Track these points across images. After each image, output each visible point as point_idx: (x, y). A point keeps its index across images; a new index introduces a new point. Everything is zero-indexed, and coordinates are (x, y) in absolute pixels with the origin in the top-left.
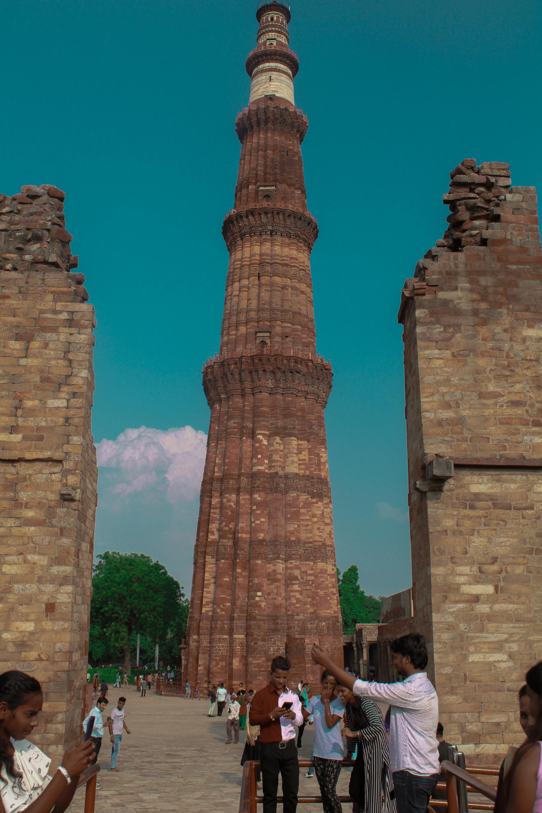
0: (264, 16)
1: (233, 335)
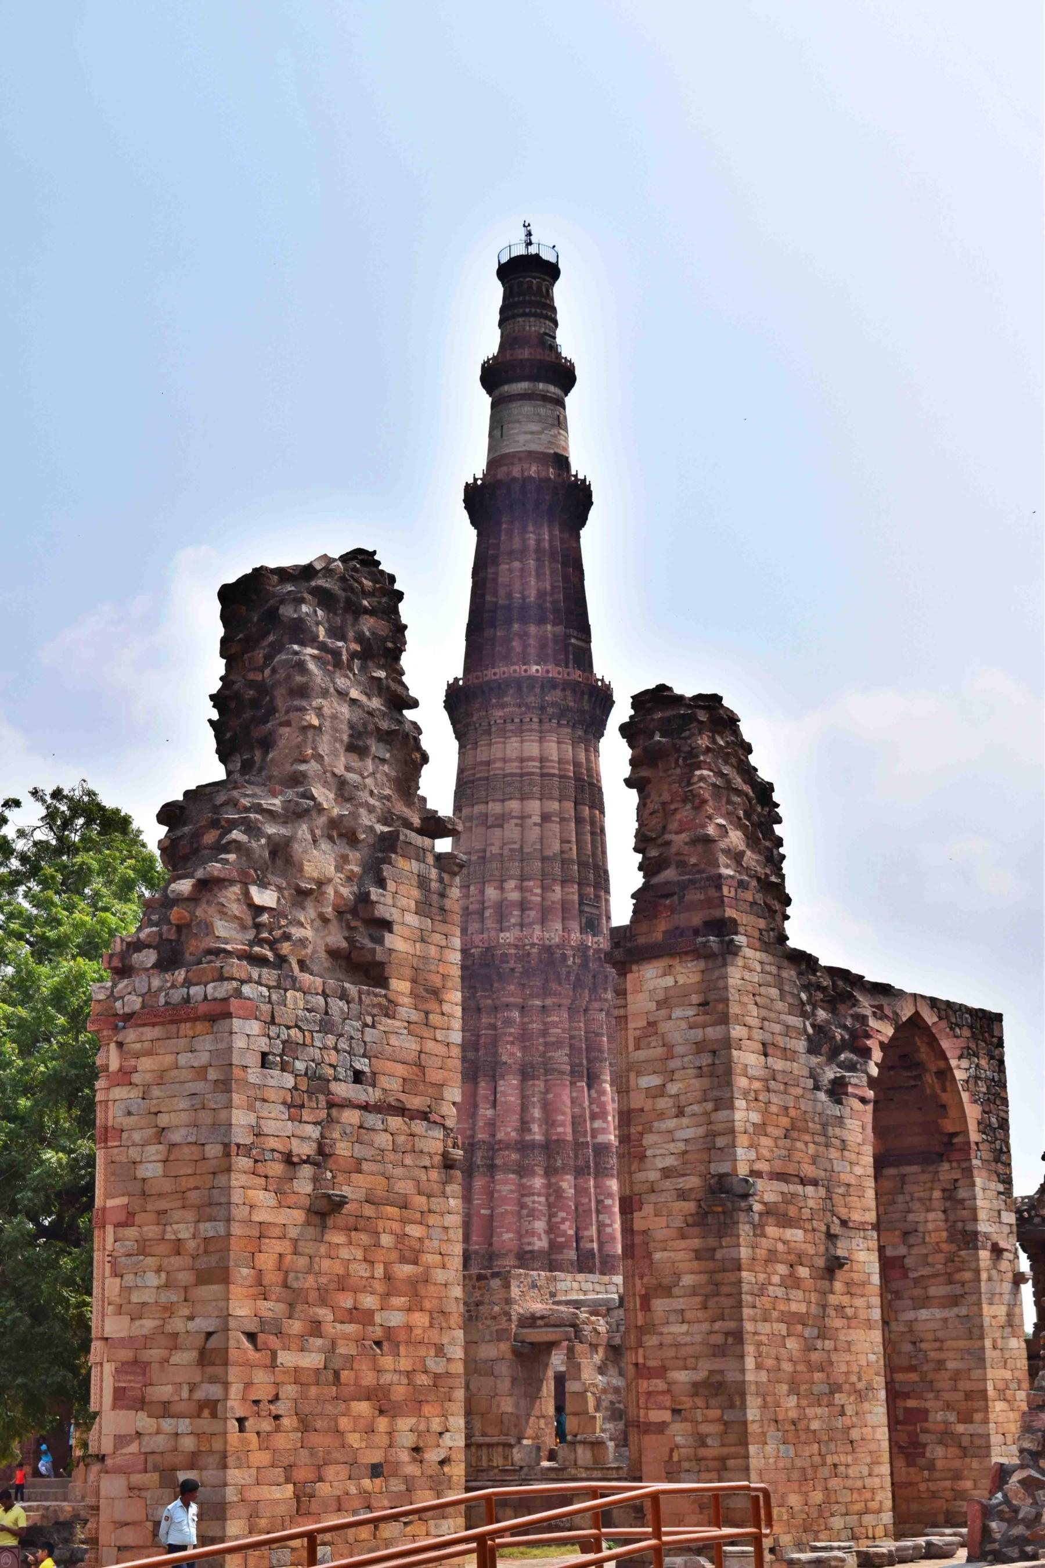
0: (535, 278)
1: (536, 895)
